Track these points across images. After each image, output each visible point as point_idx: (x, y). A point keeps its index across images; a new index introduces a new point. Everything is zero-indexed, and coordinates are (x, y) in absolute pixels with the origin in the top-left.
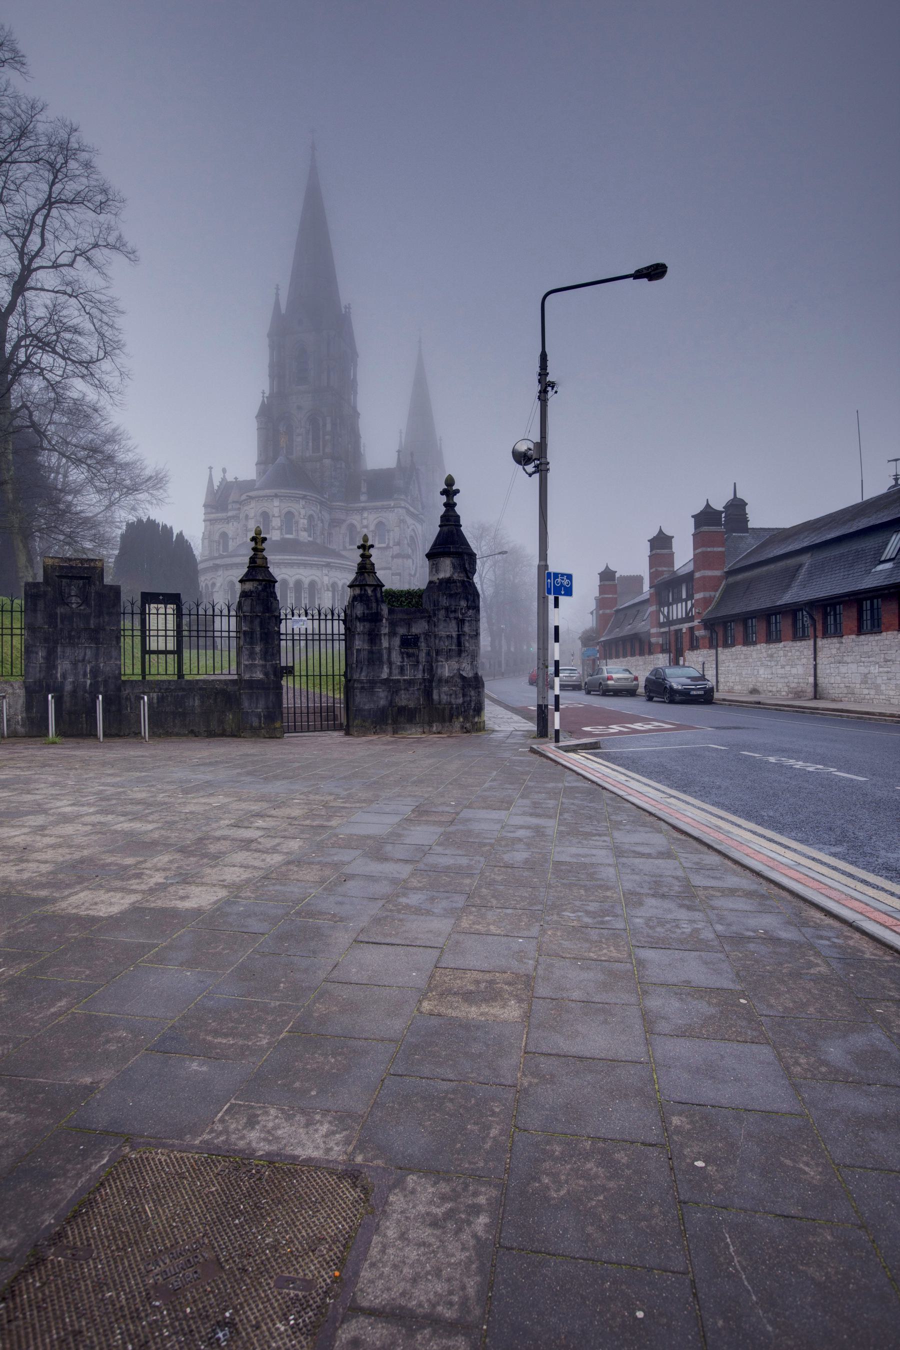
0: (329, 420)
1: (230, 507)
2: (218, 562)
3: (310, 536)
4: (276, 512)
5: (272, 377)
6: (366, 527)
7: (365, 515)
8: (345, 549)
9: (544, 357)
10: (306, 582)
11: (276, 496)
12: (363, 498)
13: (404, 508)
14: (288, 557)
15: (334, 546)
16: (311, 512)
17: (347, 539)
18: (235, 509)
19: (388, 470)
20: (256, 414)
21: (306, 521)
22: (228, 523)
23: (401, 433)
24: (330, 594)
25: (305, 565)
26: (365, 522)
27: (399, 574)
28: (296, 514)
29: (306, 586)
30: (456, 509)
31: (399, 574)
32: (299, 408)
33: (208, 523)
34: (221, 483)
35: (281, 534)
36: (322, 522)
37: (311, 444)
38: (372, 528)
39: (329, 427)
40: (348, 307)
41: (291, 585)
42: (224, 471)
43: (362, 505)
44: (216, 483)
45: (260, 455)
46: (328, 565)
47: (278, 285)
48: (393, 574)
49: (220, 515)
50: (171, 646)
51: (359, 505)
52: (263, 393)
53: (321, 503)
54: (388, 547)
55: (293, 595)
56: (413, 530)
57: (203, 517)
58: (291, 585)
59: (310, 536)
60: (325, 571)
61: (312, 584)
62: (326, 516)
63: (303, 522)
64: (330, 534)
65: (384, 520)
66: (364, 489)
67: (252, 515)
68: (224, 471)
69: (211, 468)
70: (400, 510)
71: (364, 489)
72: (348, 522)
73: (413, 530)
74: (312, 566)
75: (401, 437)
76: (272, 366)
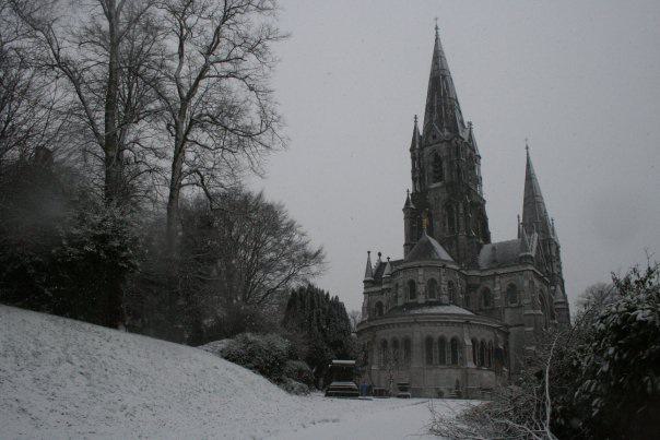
4: (421, 279)
5: (414, 179)
7: (497, 279)
16: (449, 279)
17: (483, 301)
29: (449, 341)
37: (447, 226)
38: (504, 290)
40: (470, 124)
41: (436, 340)
42: (380, 254)
44: (374, 263)
45: (406, 239)
54: (520, 306)
58: (436, 340)
61: (453, 340)
68: (380, 254)
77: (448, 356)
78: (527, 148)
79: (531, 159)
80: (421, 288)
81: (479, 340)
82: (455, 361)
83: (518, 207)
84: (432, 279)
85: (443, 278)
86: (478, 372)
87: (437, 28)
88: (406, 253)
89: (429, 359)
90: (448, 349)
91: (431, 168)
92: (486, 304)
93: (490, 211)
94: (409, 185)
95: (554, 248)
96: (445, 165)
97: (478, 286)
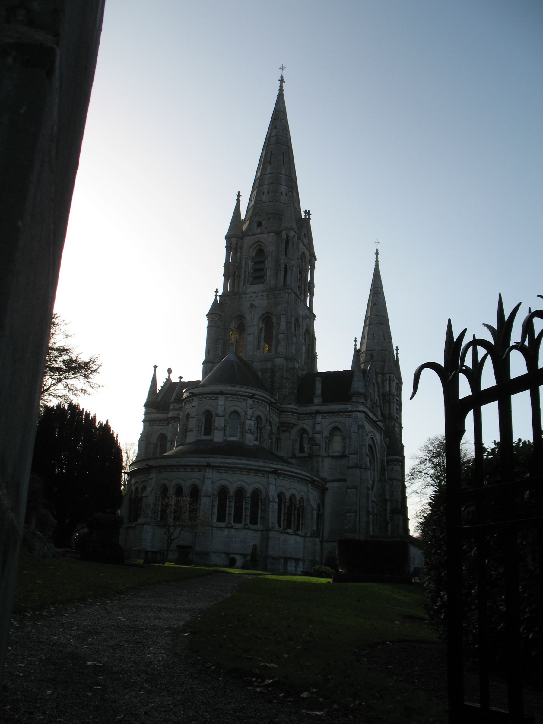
0: (283, 319)
1: (171, 407)
2: (151, 463)
3: (256, 440)
5: (227, 275)
6: (319, 433)
7: (319, 418)
8: (294, 456)
10: (249, 490)
11: (221, 393)
13: (363, 412)
14: (230, 461)
15: (281, 453)
16: (258, 413)
17: (297, 446)
18: (177, 410)
19: (345, 372)
20: (207, 311)
21: (252, 422)
22: (168, 424)
23: (356, 341)
24: (276, 506)
25: (249, 471)
26: (318, 428)
27: (356, 488)
28: (242, 414)
29: (249, 495)
31: (356, 488)
32: (252, 306)
33: (148, 423)
34: (165, 383)
35: (225, 435)
36: (271, 425)
38: (326, 433)
39: (283, 326)
40: (308, 213)
41: (232, 493)
42: (170, 371)
43: (316, 408)
44: (160, 384)
46: (275, 472)
47: (239, 192)
48: (348, 488)
51: (312, 408)
52: (217, 292)
53: (270, 404)
55: (233, 504)
56: (372, 438)
57: (143, 417)
58: (232, 493)
59: (256, 440)
60: (272, 480)
61: (256, 493)
62: (275, 419)
63: (250, 423)
64: (278, 440)
65: (340, 426)
67: (193, 414)
68: (170, 371)
69: (155, 367)
70: (358, 414)
71: (319, 392)
72: (298, 428)
73: (372, 438)
74: (256, 471)
75: (356, 345)
76: (227, 266)
77: (247, 513)
78: (377, 254)
80: (219, 422)
81: (288, 494)
82: (254, 521)
84: (235, 412)
85: (250, 412)
86: (283, 536)
87: (282, 81)
88: (205, 373)
89: (221, 518)
90: (247, 506)
91: (251, 264)
92: (302, 450)
95: (394, 385)
96: (269, 264)
97: (295, 425)
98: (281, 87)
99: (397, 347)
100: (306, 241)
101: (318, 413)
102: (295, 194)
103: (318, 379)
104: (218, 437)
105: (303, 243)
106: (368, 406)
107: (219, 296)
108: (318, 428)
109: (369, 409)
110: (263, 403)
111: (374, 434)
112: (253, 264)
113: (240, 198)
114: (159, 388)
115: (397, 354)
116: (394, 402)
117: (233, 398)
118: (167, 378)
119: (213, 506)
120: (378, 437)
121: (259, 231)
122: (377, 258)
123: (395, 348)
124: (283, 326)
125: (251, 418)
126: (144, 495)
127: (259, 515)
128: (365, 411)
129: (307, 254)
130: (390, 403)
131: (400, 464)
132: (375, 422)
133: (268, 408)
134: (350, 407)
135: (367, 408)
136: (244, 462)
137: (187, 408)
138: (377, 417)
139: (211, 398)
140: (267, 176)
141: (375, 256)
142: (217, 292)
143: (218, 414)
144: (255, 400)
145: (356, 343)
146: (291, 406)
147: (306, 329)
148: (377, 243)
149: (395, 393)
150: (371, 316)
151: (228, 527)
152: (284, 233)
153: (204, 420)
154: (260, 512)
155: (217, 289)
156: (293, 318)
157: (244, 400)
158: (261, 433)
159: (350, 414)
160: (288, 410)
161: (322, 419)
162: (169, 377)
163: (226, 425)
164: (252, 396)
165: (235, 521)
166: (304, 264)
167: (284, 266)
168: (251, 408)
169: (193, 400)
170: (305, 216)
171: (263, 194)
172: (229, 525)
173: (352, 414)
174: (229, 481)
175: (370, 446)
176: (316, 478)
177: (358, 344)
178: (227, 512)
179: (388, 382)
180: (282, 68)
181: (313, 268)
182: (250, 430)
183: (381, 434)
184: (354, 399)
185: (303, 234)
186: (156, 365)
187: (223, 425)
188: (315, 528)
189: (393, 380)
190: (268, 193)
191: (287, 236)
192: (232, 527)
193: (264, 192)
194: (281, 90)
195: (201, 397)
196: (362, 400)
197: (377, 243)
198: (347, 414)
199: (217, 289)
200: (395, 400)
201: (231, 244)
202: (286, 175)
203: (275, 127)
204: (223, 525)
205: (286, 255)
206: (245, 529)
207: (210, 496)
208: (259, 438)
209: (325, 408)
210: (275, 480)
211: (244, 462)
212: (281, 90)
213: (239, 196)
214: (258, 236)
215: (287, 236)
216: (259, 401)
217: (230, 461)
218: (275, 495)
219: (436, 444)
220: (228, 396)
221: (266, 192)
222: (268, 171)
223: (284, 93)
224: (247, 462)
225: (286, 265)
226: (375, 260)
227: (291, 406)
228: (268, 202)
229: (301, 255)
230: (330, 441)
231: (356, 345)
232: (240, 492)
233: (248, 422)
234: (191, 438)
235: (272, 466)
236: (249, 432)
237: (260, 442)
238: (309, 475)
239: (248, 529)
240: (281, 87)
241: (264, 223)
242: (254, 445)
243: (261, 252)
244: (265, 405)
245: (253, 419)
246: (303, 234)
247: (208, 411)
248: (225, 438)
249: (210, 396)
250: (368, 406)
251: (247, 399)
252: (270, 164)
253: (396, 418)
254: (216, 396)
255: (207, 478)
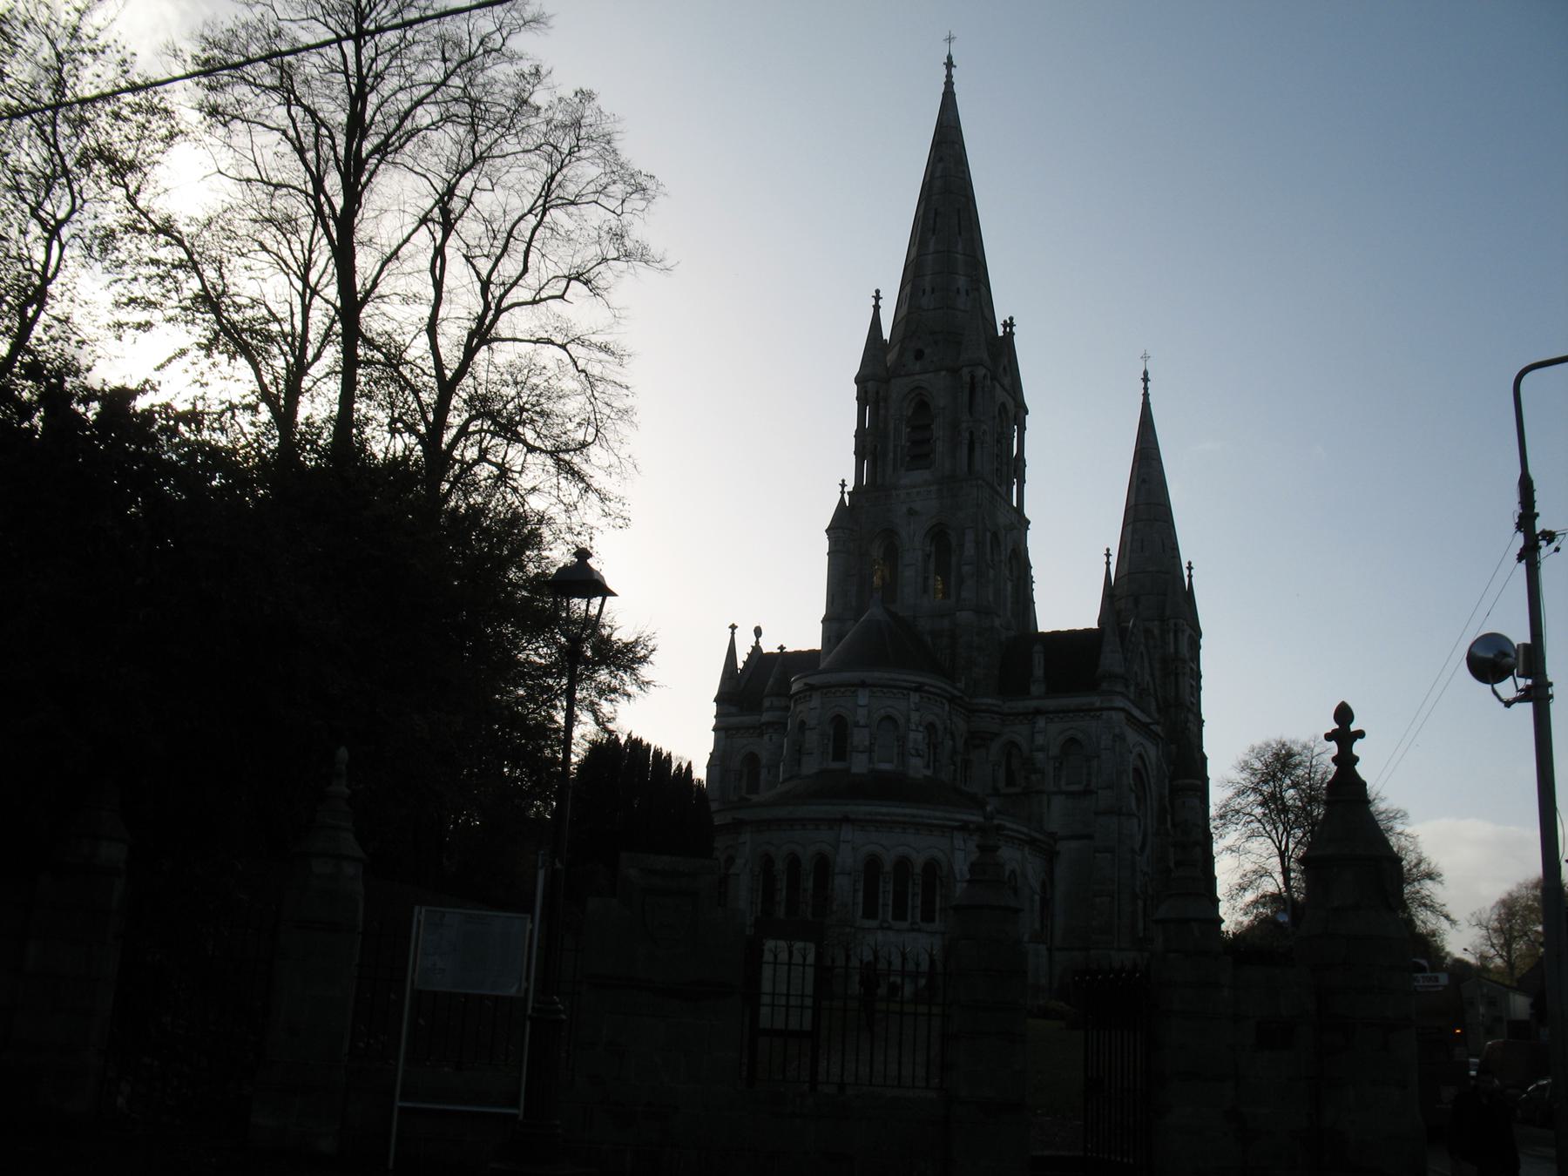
1: (767, 703)
3: (927, 766)
5: (860, 454)
7: (1041, 723)
9: (1526, 488)
10: (919, 861)
11: (863, 684)
12: (1036, 689)
13: (1122, 710)
14: (884, 810)
21: (920, 736)
22: (761, 735)
23: (1108, 555)
26: (1040, 740)
29: (918, 870)
30: (1359, 768)
32: (911, 512)
34: (750, 655)
35: (871, 760)
36: (953, 739)
39: (970, 549)
40: (1009, 324)
41: (888, 867)
44: (742, 658)
47: (878, 292)
49: (747, 719)
50: (807, 1026)
52: (843, 485)
54: (1087, 792)
55: (890, 887)
56: (1140, 756)
58: (888, 867)
59: (927, 766)
61: (931, 867)
63: (917, 737)
66: (1039, 672)
69: (733, 627)
70: (1114, 714)
71: (1039, 672)
73: (1140, 756)
75: (1108, 563)
76: (860, 434)
78: (1146, 379)
79: (1151, 399)
80: (860, 738)
82: (928, 916)
83: (1107, 529)
84: (889, 718)
85: (915, 717)
87: (949, 64)
89: (870, 913)
92: (1010, 781)
93: (1039, 547)
94: (845, 467)
98: (949, 76)
99: (1190, 563)
100: (1007, 381)
101: (1038, 712)
102: (983, 289)
103: (1037, 648)
104: (859, 765)
105: (1002, 386)
106: (1132, 697)
107: (849, 493)
108: (1040, 740)
109: (1133, 703)
110: (938, 699)
111: (1144, 747)
112: (908, 430)
113: (880, 302)
114: (740, 665)
115: (1190, 576)
116: (1184, 674)
117: (884, 693)
118: (754, 645)
119: (855, 891)
120: (1152, 753)
121: (918, 366)
122: (1146, 389)
123: (1185, 565)
124: (970, 549)
125: (917, 727)
126: (731, 871)
127: (938, 906)
128: (1127, 708)
129: (1011, 405)
130: (1177, 675)
131: (1199, 794)
132: (1146, 725)
133: (947, 707)
134: (1097, 701)
135: (1129, 699)
136: (908, 811)
137: (800, 712)
138: (1149, 715)
139: (843, 693)
140: (930, 257)
141: (1143, 384)
142: (843, 485)
143: (858, 722)
144: (924, 695)
145: (1108, 558)
146: (990, 701)
147: (1013, 550)
148: (1145, 357)
149: (1187, 656)
150: (1136, 505)
151: (882, 928)
152: (965, 371)
153: (832, 732)
154: (938, 899)
155: (843, 481)
156: (988, 534)
157: (904, 695)
158: (935, 754)
159: (1098, 714)
160: (984, 707)
161: (1046, 723)
162: (757, 642)
163: (873, 742)
164: (919, 688)
165: (895, 918)
166: (1005, 424)
167: (967, 435)
168: (917, 710)
169: (810, 696)
170: (1005, 331)
171: (924, 294)
172: (886, 925)
173: (1101, 714)
174: (881, 845)
175: (1136, 770)
176: (1037, 835)
177: (1114, 560)
178: (881, 901)
179: (1172, 635)
180: (950, 39)
181: (1022, 429)
182: (917, 750)
183: (1157, 745)
184: (1105, 686)
185: (1001, 369)
186: (733, 624)
187: (867, 743)
188: (1037, 926)
189: (1183, 631)
190: (933, 290)
191: (973, 377)
192: (889, 928)
193: (924, 290)
194: (949, 84)
195: (825, 691)
196: (1119, 688)
197: (1145, 357)
198: (1092, 714)
199: (843, 481)
200: (1188, 670)
201: (866, 392)
202: (964, 254)
203: (941, 160)
204: (873, 923)
205: (971, 413)
206: (913, 930)
207: (850, 874)
208: (931, 764)
209: (1051, 703)
210: (964, 841)
211: (908, 811)
212: (949, 84)
213: (877, 297)
214: (917, 377)
215: (973, 377)
216: (931, 697)
217: (884, 810)
218: (965, 868)
219: (1268, 757)
220: (875, 689)
221: (928, 289)
222: (931, 248)
223: (956, 88)
224: (915, 811)
225: (971, 433)
226: (1143, 392)
227: (990, 701)
228: (934, 309)
229: (999, 410)
230: (1061, 763)
231: (1108, 563)
232: (903, 864)
233: (912, 735)
234: (810, 766)
235: (958, 816)
236: (913, 752)
237: (934, 768)
238: (1025, 830)
239: (919, 930)
240: (949, 76)
241: (927, 351)
242: (925, 776)
243: (923, 406)
244: (942, 703)
245: (921, 729)
246: (1001, 369)
247: (839, 716)
248: (871, 766)
249: (842, 690)
250: (1132, 697)
251: (909, 694)
252: (934, 234)
253: (1189, 704)
254: (853, 689)
255: (844, 842)
